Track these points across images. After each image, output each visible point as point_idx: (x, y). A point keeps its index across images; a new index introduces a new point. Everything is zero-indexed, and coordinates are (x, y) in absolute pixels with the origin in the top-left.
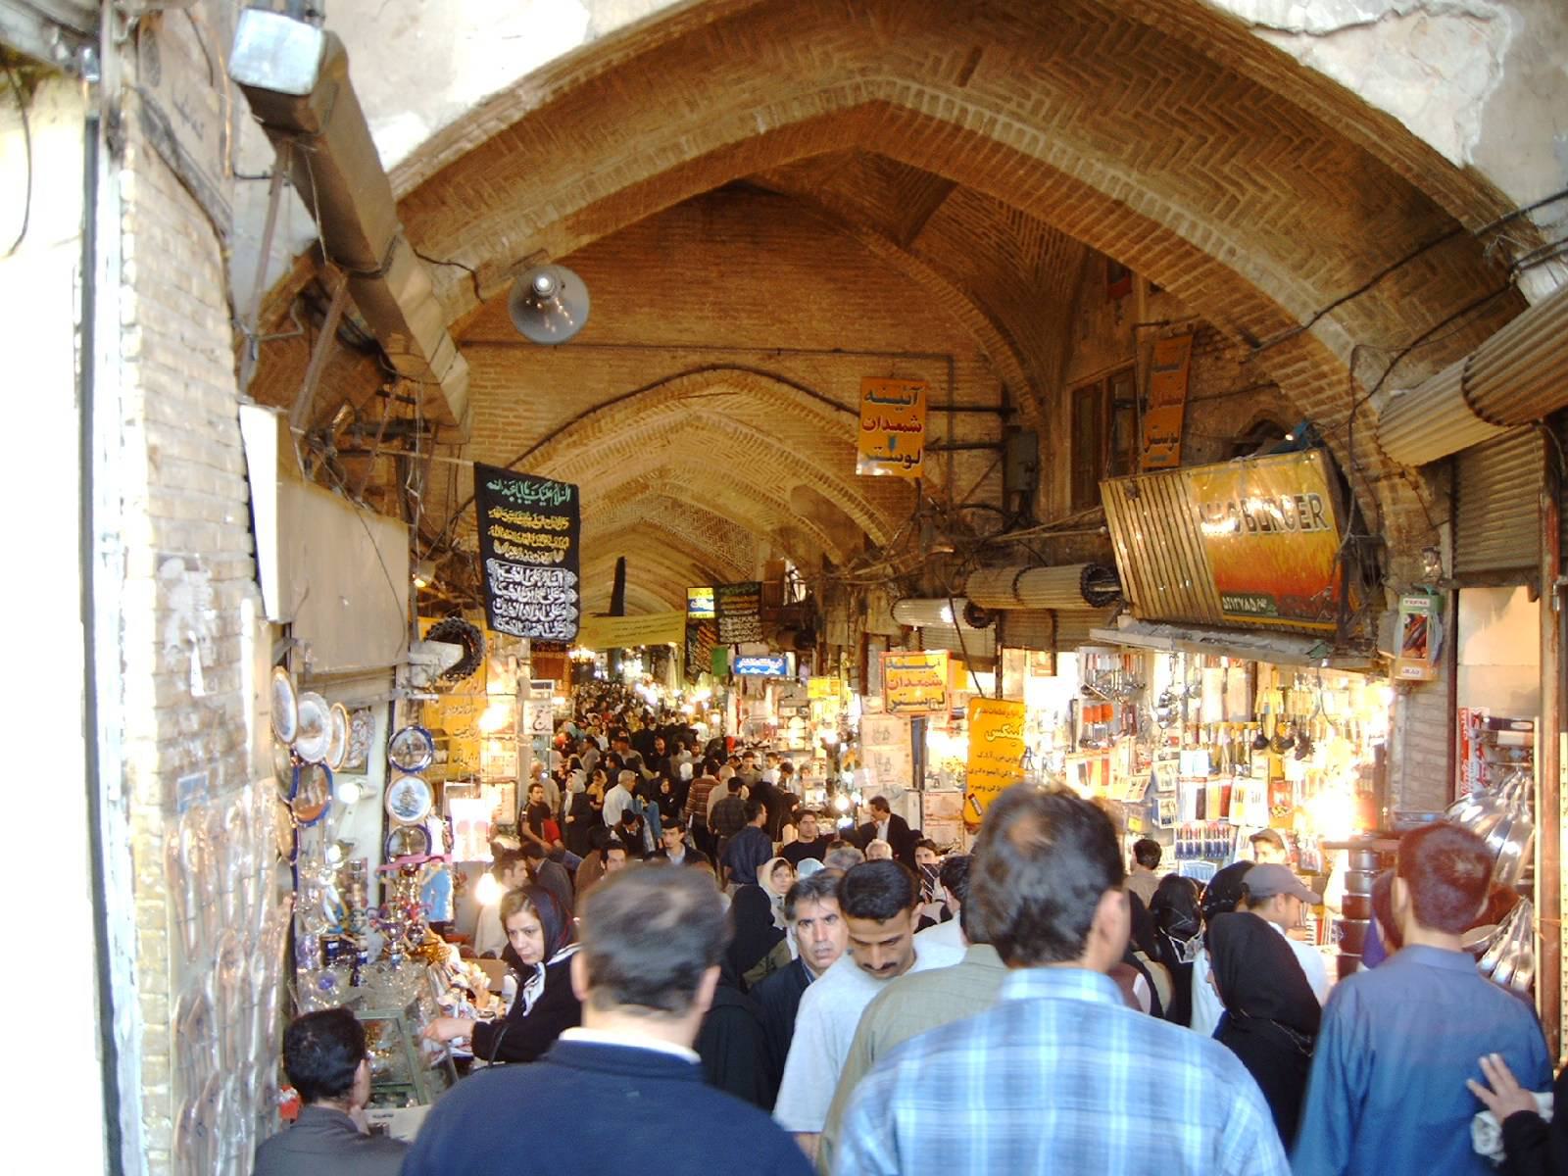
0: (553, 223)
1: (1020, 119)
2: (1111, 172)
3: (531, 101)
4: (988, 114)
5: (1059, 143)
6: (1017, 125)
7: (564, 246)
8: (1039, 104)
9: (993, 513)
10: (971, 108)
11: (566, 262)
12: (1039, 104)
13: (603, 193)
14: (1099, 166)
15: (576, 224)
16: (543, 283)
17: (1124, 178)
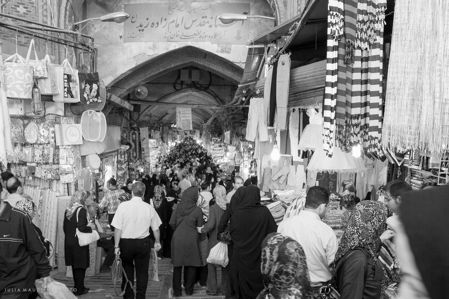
0: (140, 82)
1: (214, 64)
2: (229, 72)
3: (130, 72)
4: (209, 63)
5: (221, 68)
6: (214, 65)
7: (143, 83)
8: (217, 62)
9: (242, 116)
10: (206, 62)
11: (143, 85)
12: (217, 62)
13: (147, 77)
14: (227, 72)
15: (144, 81)
16: (139, 90)
17: (231, 74)
